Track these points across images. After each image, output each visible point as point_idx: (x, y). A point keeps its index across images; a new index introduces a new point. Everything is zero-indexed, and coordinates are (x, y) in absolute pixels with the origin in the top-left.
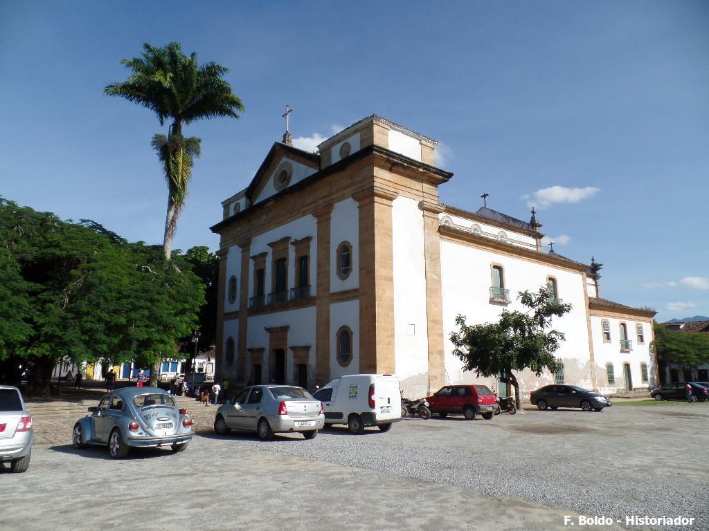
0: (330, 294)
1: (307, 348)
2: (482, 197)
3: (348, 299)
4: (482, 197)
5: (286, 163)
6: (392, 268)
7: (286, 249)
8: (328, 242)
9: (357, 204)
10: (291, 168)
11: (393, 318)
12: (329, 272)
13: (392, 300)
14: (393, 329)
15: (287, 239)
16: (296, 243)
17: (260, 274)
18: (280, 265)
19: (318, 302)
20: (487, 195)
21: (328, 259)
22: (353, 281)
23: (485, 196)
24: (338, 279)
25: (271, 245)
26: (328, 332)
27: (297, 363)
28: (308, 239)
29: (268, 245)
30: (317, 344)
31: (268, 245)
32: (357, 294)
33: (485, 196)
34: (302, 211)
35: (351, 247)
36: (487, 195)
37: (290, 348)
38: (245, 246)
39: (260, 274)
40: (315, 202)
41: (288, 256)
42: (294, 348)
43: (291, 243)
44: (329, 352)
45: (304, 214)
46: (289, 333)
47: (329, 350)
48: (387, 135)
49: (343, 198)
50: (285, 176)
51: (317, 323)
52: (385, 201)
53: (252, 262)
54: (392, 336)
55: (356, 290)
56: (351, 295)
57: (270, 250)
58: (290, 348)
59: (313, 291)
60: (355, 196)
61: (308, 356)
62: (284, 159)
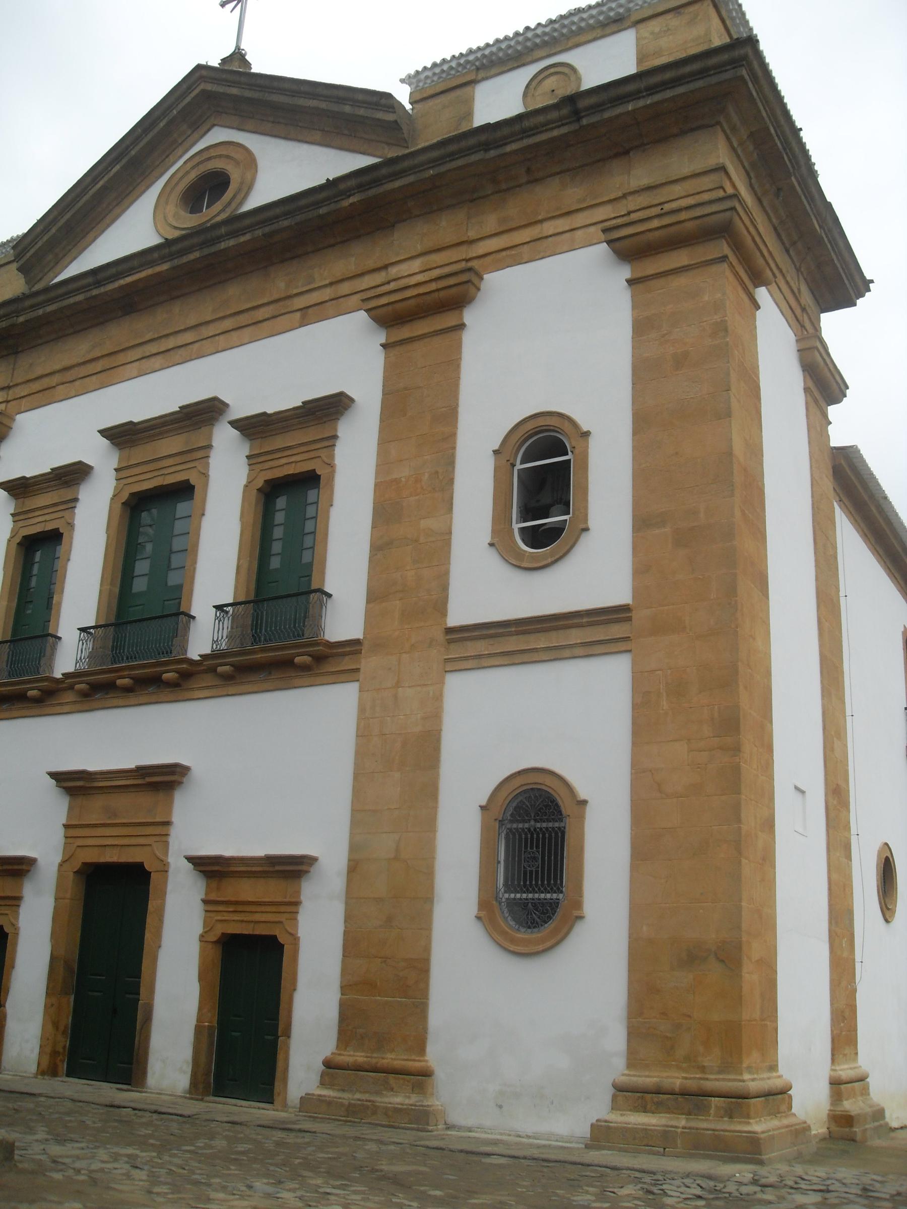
0: (450, 631)
9: (625, 272)
10: (250, 162)
12: (445, 538)
19: (368, 663)
29: (104, 433)
30: (354, 848)
31: (104, 433)
32: (617, 630)
34: (300, 302)
37: (190, 859)
40: (385, 267)
41: (205, 475)
43: (235, 424)
44: (431, 887)
47: (429, 874)
51: (361, 754)
56: (575, 636)
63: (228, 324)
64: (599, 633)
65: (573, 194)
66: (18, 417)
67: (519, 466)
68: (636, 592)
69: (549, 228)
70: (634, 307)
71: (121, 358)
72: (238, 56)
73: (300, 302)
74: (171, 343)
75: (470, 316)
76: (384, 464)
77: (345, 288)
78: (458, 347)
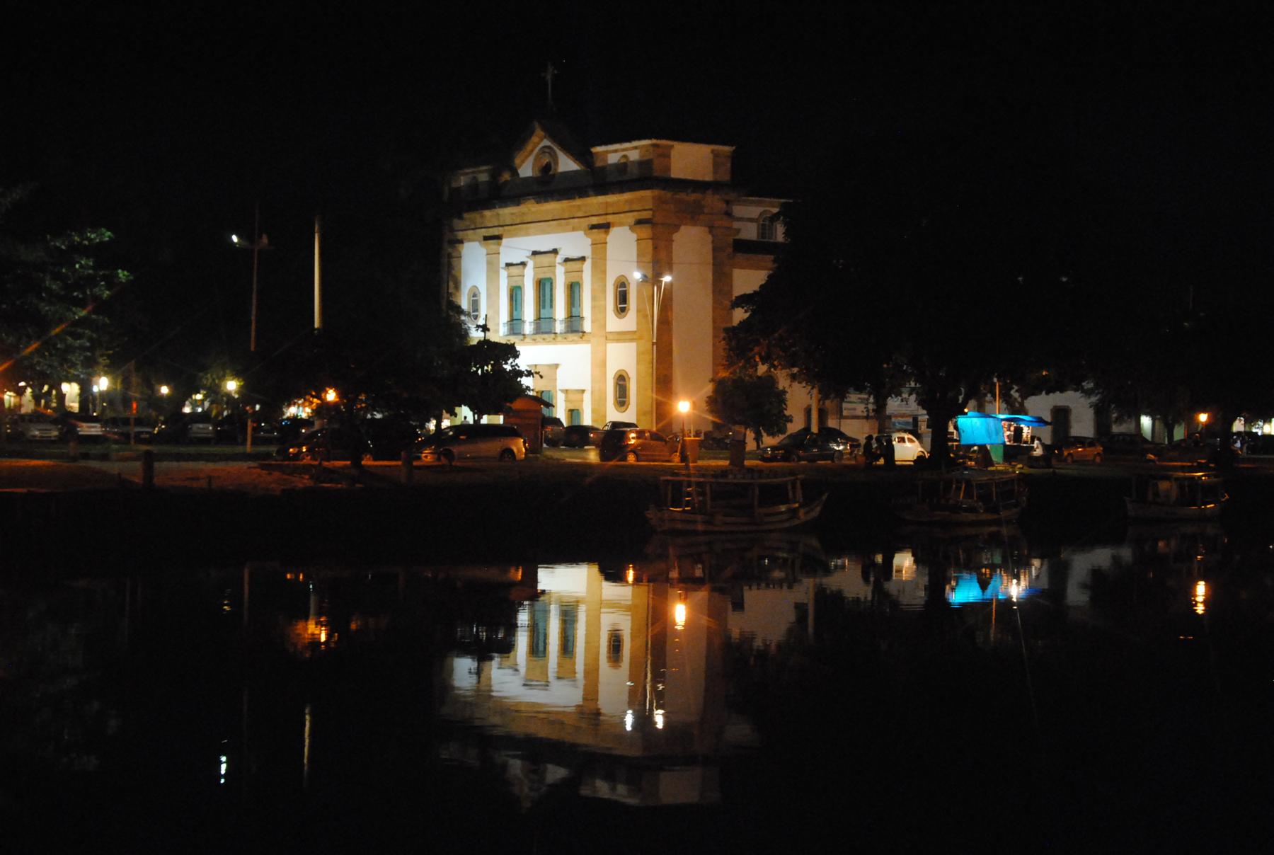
1: (583, 391)
3: (624, 341)
5: (549, 147)
7: (553, 266)
8: (604, 272)
24: (614, 315)
26: (605, 374)
27: (570, 408)
30: (592, 387)
35: (629, 284)
37: (560, 390)
41: (555, 276)
42: (566, 392)
46: (558, 370)
53: (503, 274)
58: (560, 390)
59: (587, 326)
61: (582, 401)
67: (619, 289)
68: (637, 328)
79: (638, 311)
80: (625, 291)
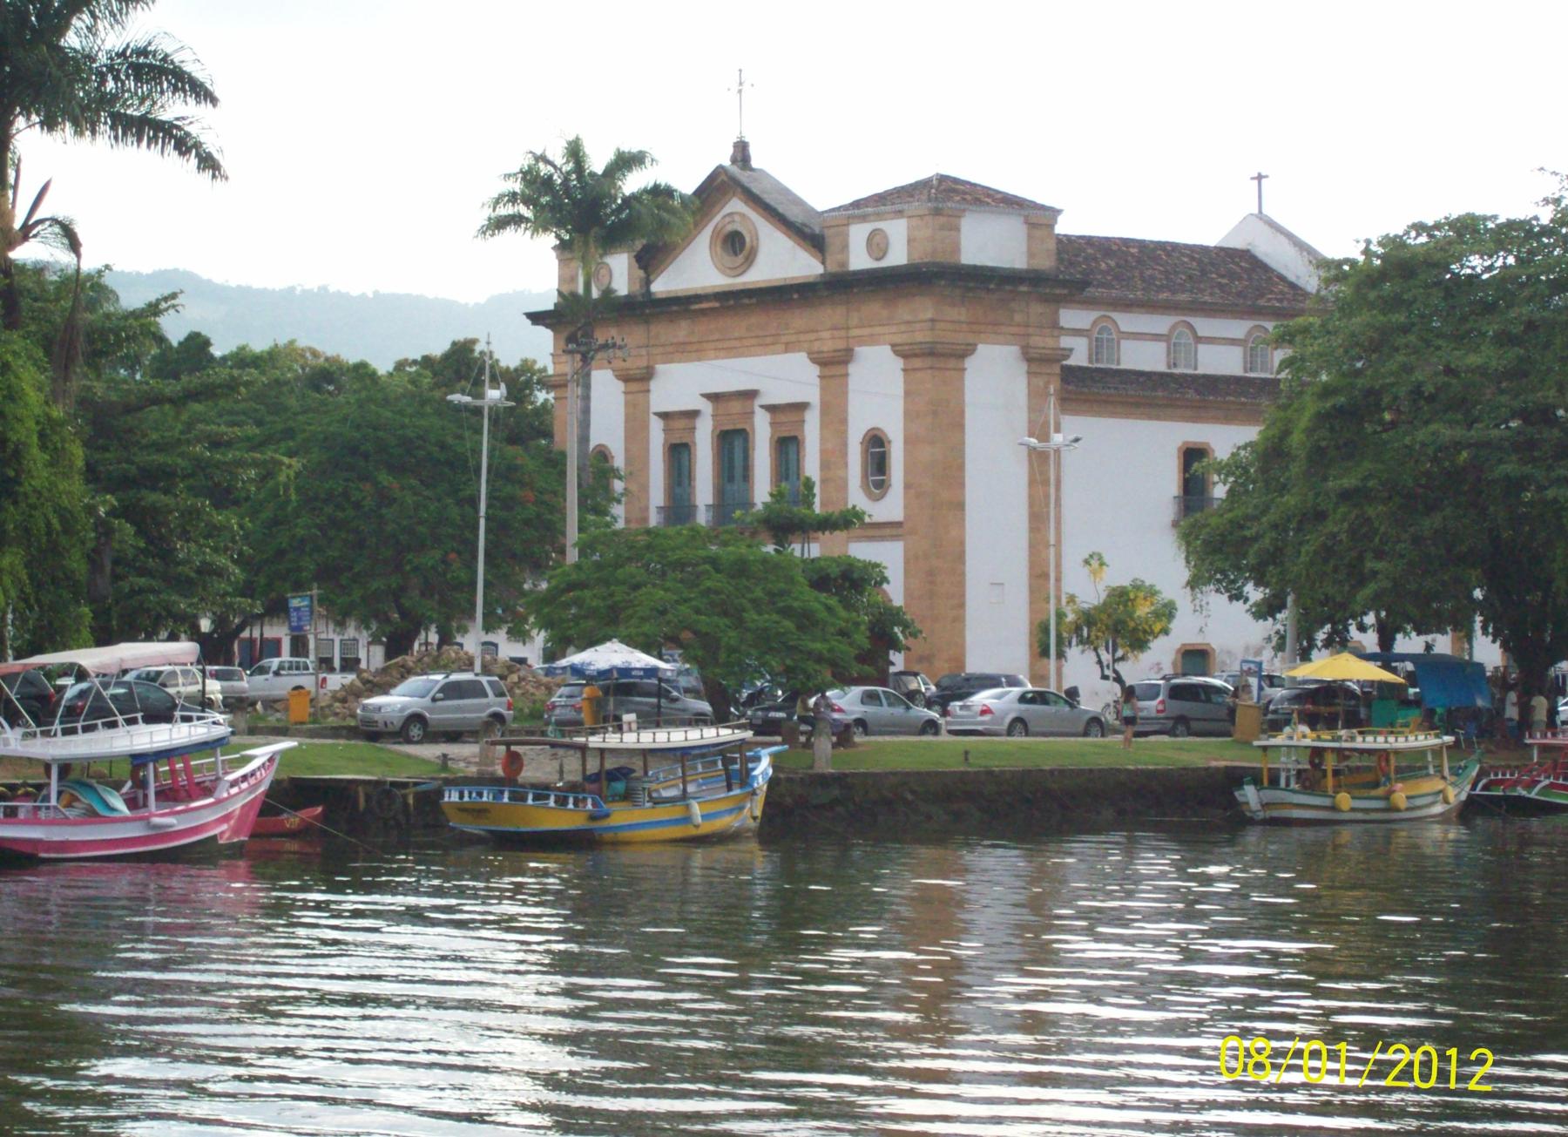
2: (1253, 178)
3: (882, 538)
4: (1253, 178)
6: (962, 485)
8: (844, 421)
11: (963, 574)
13: (962, 543)
14: (963, 595)
15: (751, 395)
16: (772, 409)
17: (679, 454)
18: (732, 443)
20: (1266, 177)
21: (844, 454)
22: (891, 507)
23: (1260, 178)
25: (714, 398)
28: (801, 407)
31: (704, 395)
32: (900, 531)
33: (1260, 178)
36: (1266, 177)
38: (638, 380)
39: (679, 454)
41: (752, 425)
45: (789, 348)
48: (958, 229)
49: (872, 340)
50: (735, 245)
52: (952, 363)
54: (962, 605)
55: (898, 524)
56: (888, 531)
57: (706, 407)
60: (897, 348)
62: (736, 205)
63: (754, 341)
64: (894, 532)
65: (885, 313)
66: (657, 366)
68: (907, 516)
69: (878, 330)
70: (905, 382)
71: (705, 345)
72: (742, 152)
73: (784, 339)
74: (727, 344)
75: (852, 368)
76: (823, 439)
77: (802, 337)
78: (846, 385)
79: (907, 486)
80: (884, 453)
